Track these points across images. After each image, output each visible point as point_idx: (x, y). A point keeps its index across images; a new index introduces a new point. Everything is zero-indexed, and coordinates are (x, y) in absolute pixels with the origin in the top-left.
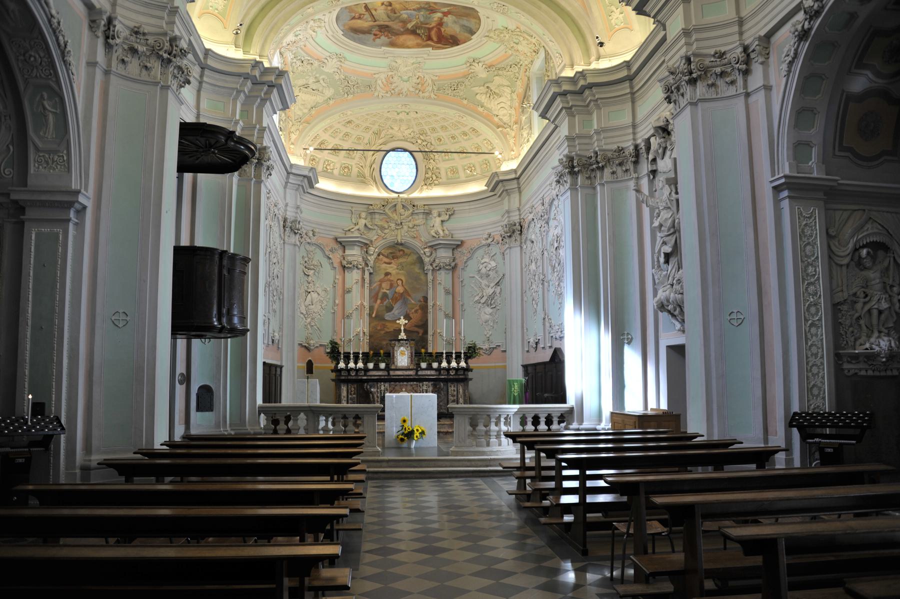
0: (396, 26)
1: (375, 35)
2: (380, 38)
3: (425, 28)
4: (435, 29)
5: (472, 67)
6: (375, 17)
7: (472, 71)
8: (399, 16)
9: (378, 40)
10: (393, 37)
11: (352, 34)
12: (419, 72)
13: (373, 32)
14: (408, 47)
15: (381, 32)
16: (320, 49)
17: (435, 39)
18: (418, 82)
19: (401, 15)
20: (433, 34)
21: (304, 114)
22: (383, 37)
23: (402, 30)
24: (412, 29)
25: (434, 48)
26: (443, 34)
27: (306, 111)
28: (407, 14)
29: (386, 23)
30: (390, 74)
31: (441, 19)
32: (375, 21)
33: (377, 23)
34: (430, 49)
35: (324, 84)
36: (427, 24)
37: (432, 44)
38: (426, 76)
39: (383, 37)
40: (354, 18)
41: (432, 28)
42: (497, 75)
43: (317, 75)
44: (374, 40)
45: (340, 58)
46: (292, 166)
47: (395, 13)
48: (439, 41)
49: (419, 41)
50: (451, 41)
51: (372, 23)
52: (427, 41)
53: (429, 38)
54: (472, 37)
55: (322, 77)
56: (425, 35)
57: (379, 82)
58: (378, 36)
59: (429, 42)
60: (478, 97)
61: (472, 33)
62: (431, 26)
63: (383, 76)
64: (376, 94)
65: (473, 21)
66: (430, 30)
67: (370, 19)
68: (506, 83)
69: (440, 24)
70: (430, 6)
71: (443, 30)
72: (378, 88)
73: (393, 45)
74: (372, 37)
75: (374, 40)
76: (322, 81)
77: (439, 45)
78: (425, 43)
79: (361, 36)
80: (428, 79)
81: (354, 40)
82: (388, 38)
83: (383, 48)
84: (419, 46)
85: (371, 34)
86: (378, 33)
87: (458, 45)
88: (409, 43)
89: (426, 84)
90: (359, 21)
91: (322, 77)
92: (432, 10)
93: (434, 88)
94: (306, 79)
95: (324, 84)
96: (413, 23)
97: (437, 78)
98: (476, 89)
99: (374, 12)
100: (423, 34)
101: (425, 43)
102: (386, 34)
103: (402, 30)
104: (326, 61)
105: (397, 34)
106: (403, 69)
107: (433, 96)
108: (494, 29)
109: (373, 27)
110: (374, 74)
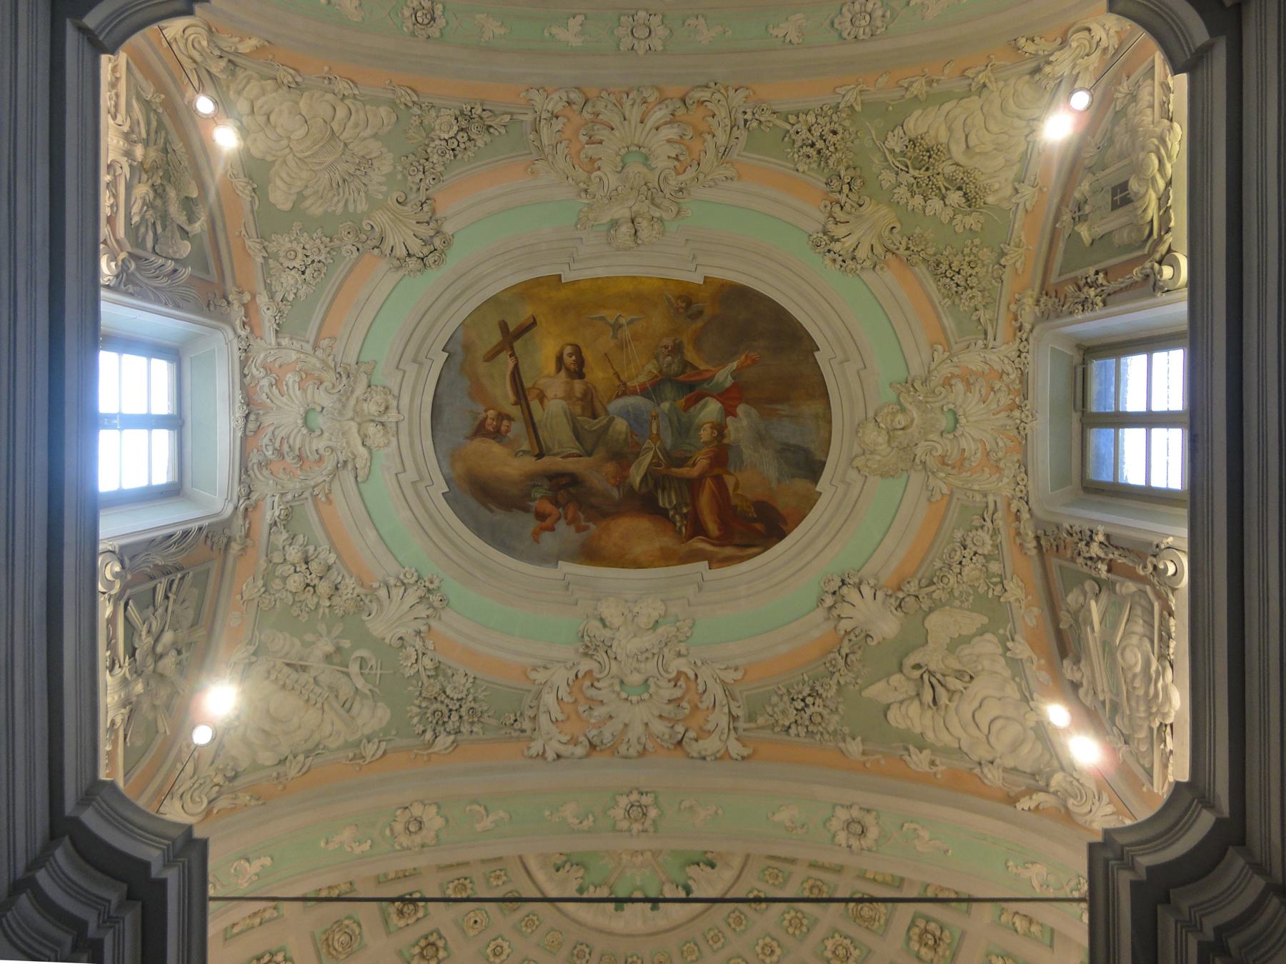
1: (541, 516)
2: (552, 529)
4: (709, 483)
5: (845, 610)
6: (542, 434)
7: (845, 625)
9: (548, 541)
10: (592, 526)
12: (679, 655)
13: (534, 504)
14: (636, 564)
15: (556, 503)
16: (371, 535)
17: (713, 528)
18: (678, 693)
19: (612, 420)
20: (705, 501)
21: (255, 767)
22: (562, 526)
23: (615, 494)
24: (644, 490)
25: (717, 562)
26: (735, 501)
27: (267, 758)
28: (625, 414)
29: (571, 465)
30: (585, 665)
31: (720, 429)
32: (540, 456)
33: (548, 463)
34: (704, 565)
35: (360, 683)
36: (682, 462)
37: (708, 547)
38: (705, 674)
39: (562, 526)
40: (480, 431)
41: (701, 478)
42: (931, 610)
43: (346, 644)
44: (536, 536)
45: (430, 595)
46: (95, 791)
47: (594, 416)
48: (722, 541)
49: (667, 541)
50: (758, 526)
51: (529, 464)
53: (697, 529)
54: (818, 489)
55: (358, 653)
56: (684, 516)
57: (549, 699)
58: (548, 522)
59: (699, 544)
60: (894, 717)
61: (812, 468)
62: (694, 472)
63: (561, 677)
64: (536, 747)
65: (810, 408)
66: (693, 486)
67: (526, 446)
68: (970, 622)
69: (722, 456)
70: (686, 364)
71: (730, 481)
72: (543, 719)
73: (591, 554)
74: (532, 523)
75: (536, 536)
76: (354, 668)
77: (729, 551)
78: (684, 548)
79: (500, 516)
80: (710, 683)
81: (479, 529)
82: (579, 530)
83: (567, 567)
84: (668, 558)
85: (526, 510)
86: (547, 507)
87: (782, 536)
88: (640, 549)
89: (707, 701)
90: (496, 449)
91: (358, 653)
92: (691, 387)
93: (735, 712)
94: (305, 644)
95: (360, 683)
96: (647, 460)
97: (739, 675)
98: (877, 691)
99: (535, 405)
100: (675, 508)
101: (684, 548)
103: (615, 494)
104: (383, 593)
105: (601, 511)
106: (628, 644)
107: (735, 748)
108: (871, 414)
109: (533, 479)
110: (535, 669)
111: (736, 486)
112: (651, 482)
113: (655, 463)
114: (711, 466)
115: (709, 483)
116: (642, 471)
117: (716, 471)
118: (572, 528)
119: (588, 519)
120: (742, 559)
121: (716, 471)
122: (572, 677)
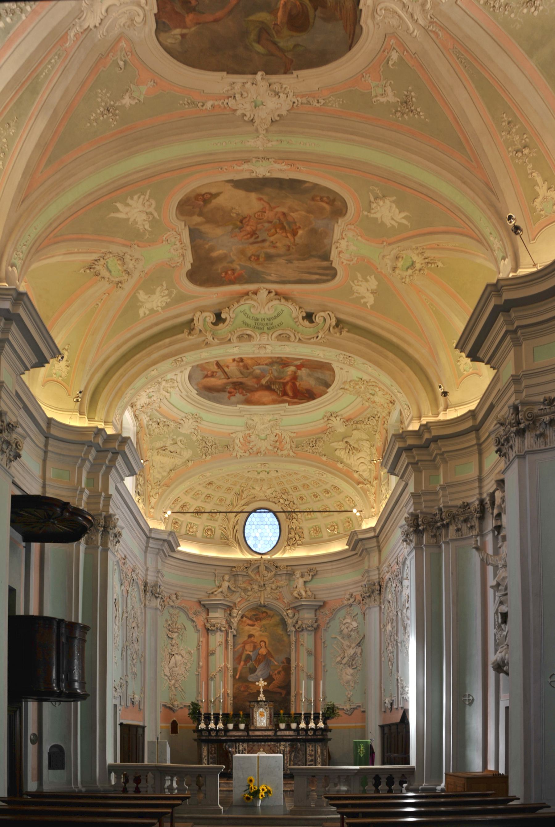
0: (250, 382)
1: (230, 393)
2: (234, 396)
3: (279, 383)
4: (290, 384)
8: (253, 372)
10: (248, 394)
11: (206, 393)
14: (264, 404)
15: (235, 389)
17: (290, 394)
20: (288, 388)
22: (238, 395)
23: (256, 386)
25: (290, 403)
26: (298, 388)
29: (240, 380)
32: (229, 378)
33: (230, 380)
36: (281, 378)
37: (288, 399)
39: (238, 395)
44: (229, 398)
48: (295, 396)
49: (275, 397)
50: (307, 395)
51: (225, 381)
52: (282, 396)
53: (285, 393)
56: (280, 391)
58: (233, 394)
59: (285, 398)
62: (285, 381)
66: (285, 384)
67: (223, 377)
71: (298, 384)
73: (248, 402)
75: (229, 398)
77: (295, 400)
79: (216, 394)
81: (209, 399)
82: (244, 395)
83: (239, 406)
84: (274, 402)
85: (225, 391)
86: (232, 390)
87: (314, 399)
101: (281, 399)
102: (240, 391)
105: (251, 390)
111: (300, 385)
112: (269, 383)
113: (271, 378)
114: (291, 380)
115: (290, 384)
116: (266, 381)
117: (293, 381)
118: (241, 395)
119: (246, 392)
120: (300, 403)
121: (293, 381)
122: (243, 435)
